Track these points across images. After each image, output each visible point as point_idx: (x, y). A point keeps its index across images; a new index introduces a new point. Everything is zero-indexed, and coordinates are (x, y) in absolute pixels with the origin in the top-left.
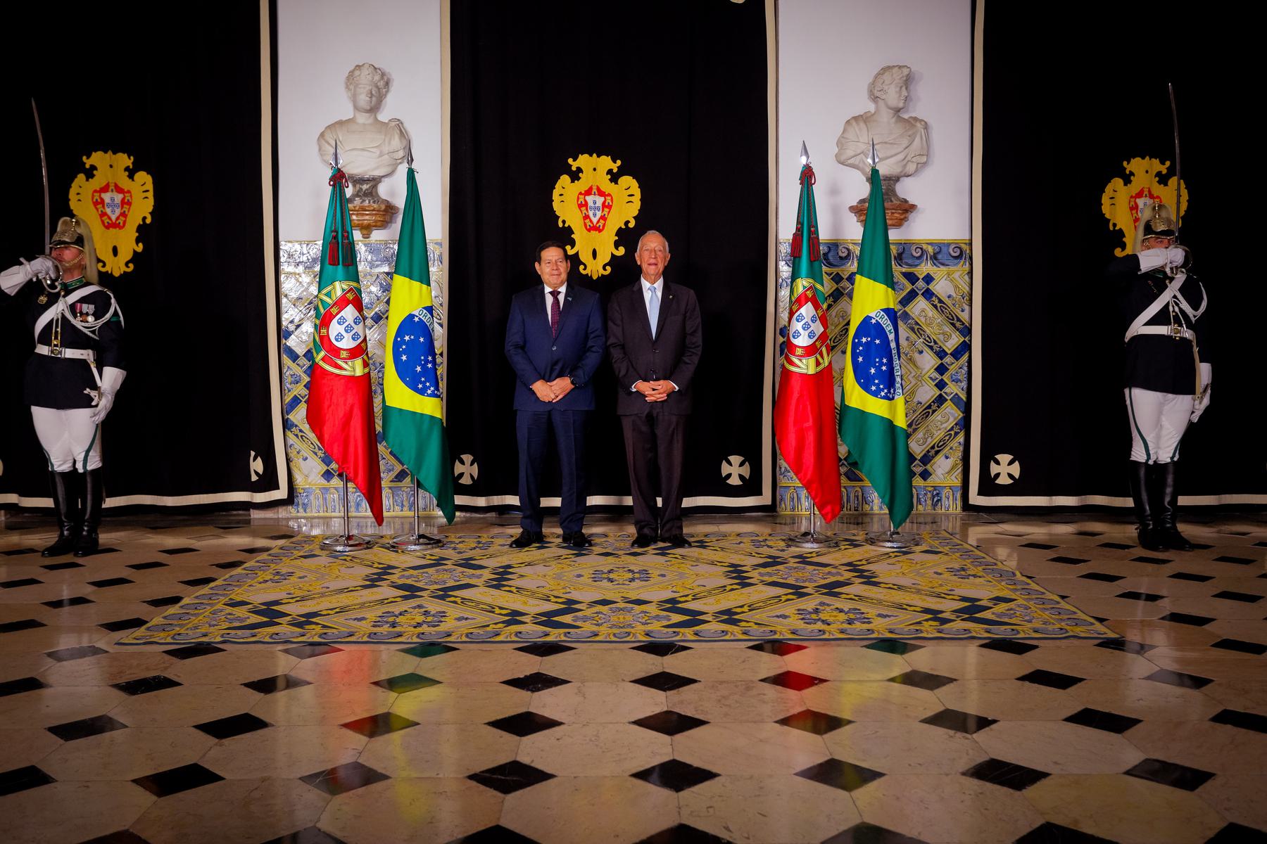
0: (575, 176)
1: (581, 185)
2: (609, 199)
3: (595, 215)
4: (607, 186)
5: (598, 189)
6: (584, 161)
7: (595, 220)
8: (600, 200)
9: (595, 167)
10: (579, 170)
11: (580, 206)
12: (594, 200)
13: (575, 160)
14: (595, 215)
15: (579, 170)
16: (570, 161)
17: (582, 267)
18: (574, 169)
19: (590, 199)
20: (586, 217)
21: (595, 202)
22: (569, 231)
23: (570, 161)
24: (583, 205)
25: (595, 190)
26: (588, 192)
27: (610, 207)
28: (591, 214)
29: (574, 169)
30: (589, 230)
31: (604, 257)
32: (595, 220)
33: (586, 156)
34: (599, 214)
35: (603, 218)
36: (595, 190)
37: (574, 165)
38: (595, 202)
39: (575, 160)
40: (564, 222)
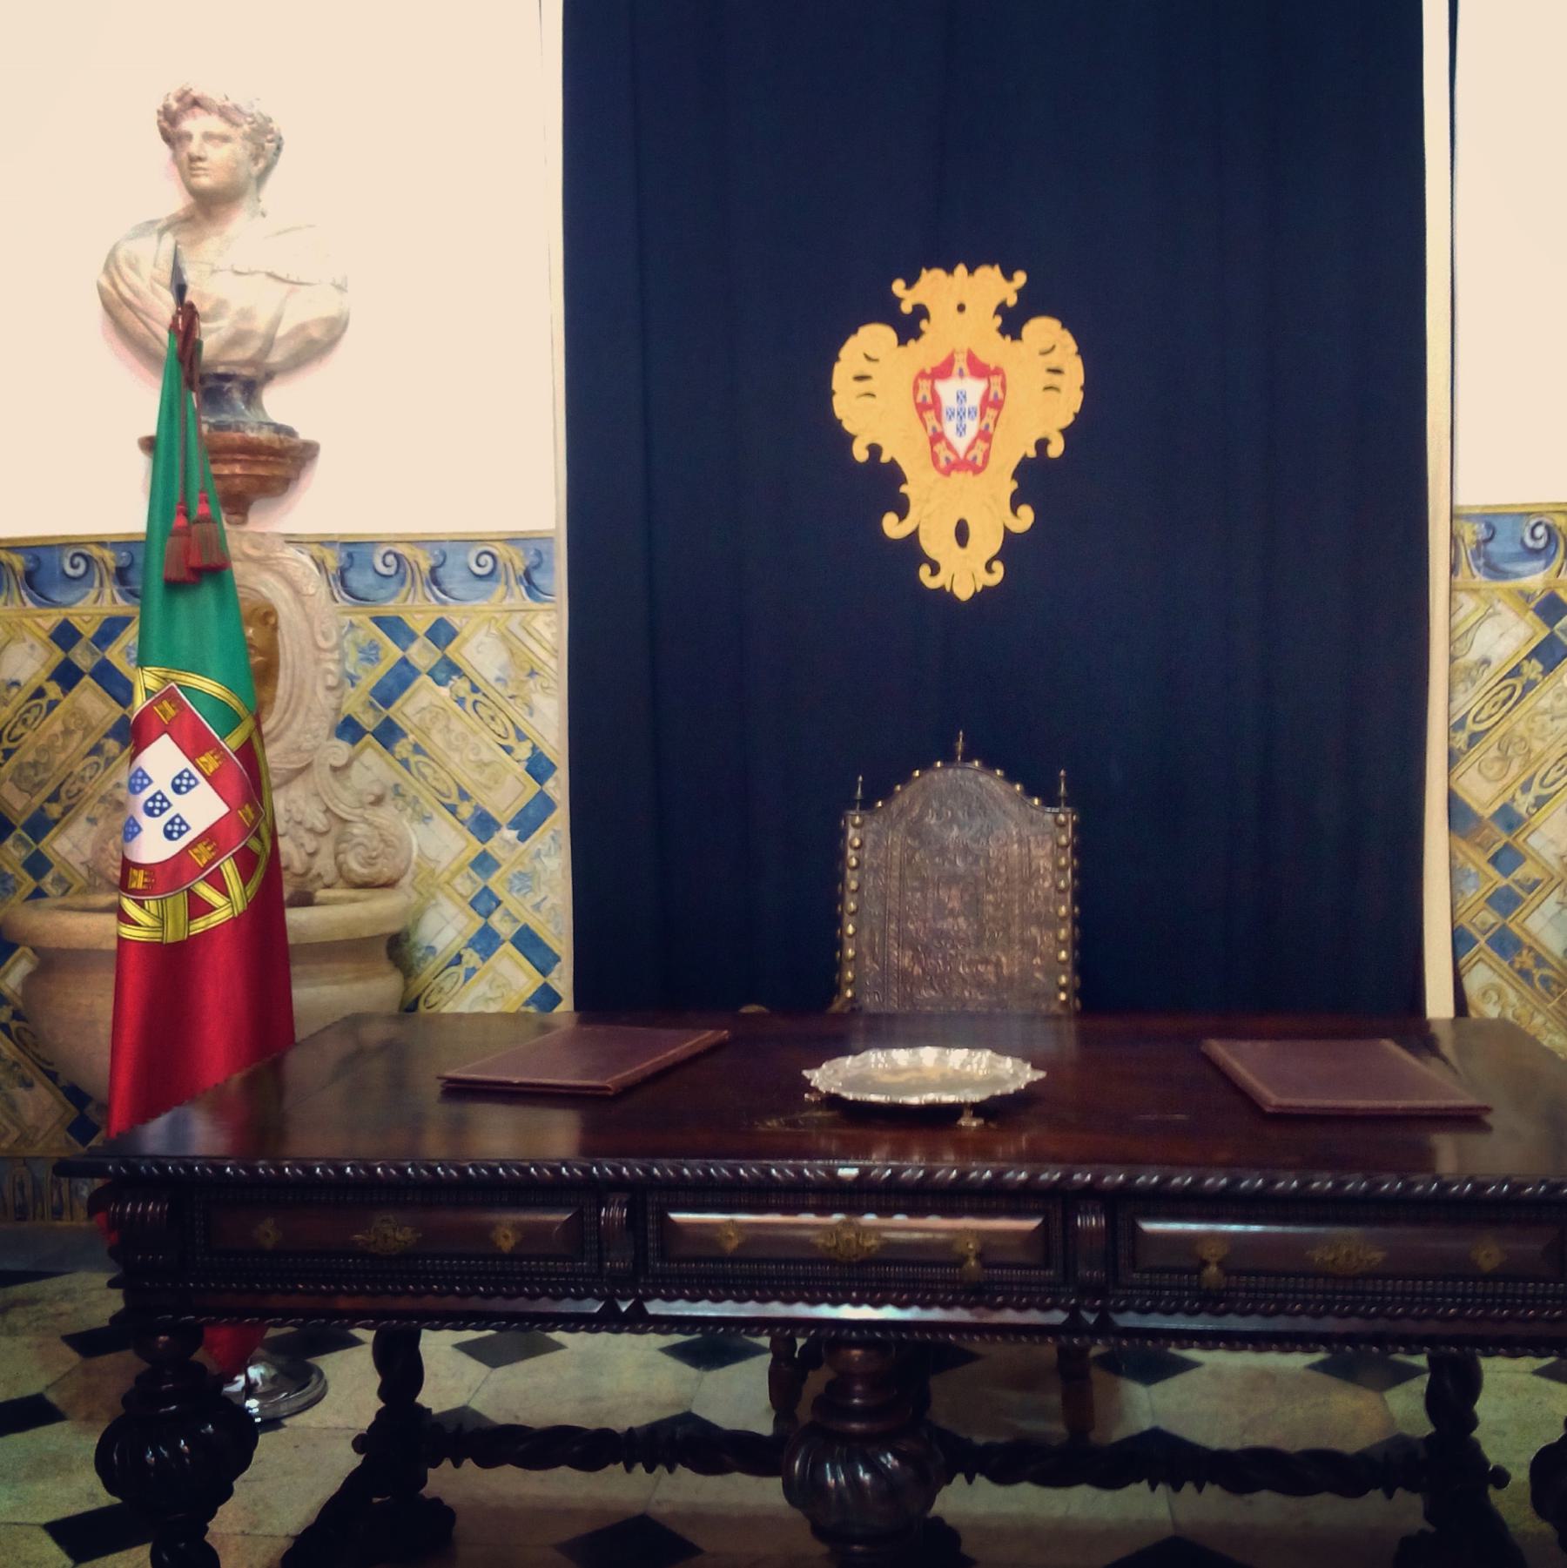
0: (909, 327)
1: (924, 352)
2: (996, 380)
3: (961, 430)
4: (995, 349)
5: (972, 359)
6: (934, 289)
7: (961, 444)
8: (975, 389)
9: (962, 299)
10: (921, 312)
11: (922, 408)
12: (960, 391)
13: (910, 284)
14: (961, 430)
15: (921, 312)
16: (898, 287)
17: (924, 571)
18: (906, 308)
19: (947, 390)
20: (937, 437)
21: (961, 397)
22: (894, 474)
23: (898, 287)
24: (929, 406)
25: (961, 363)
26: (943, 371)
27: (998, 405)
28: (950, 428)
29: (906, 308)
30: (946, 472)
31: (987, 541)
32: (961, 444)
33: (938, 273)
34: (973, 427)
35: (985, 435)
36: (961, 363)
37: (907, 297)
38: (961, 397)
39: (910, 284)
40: (875, 450)
